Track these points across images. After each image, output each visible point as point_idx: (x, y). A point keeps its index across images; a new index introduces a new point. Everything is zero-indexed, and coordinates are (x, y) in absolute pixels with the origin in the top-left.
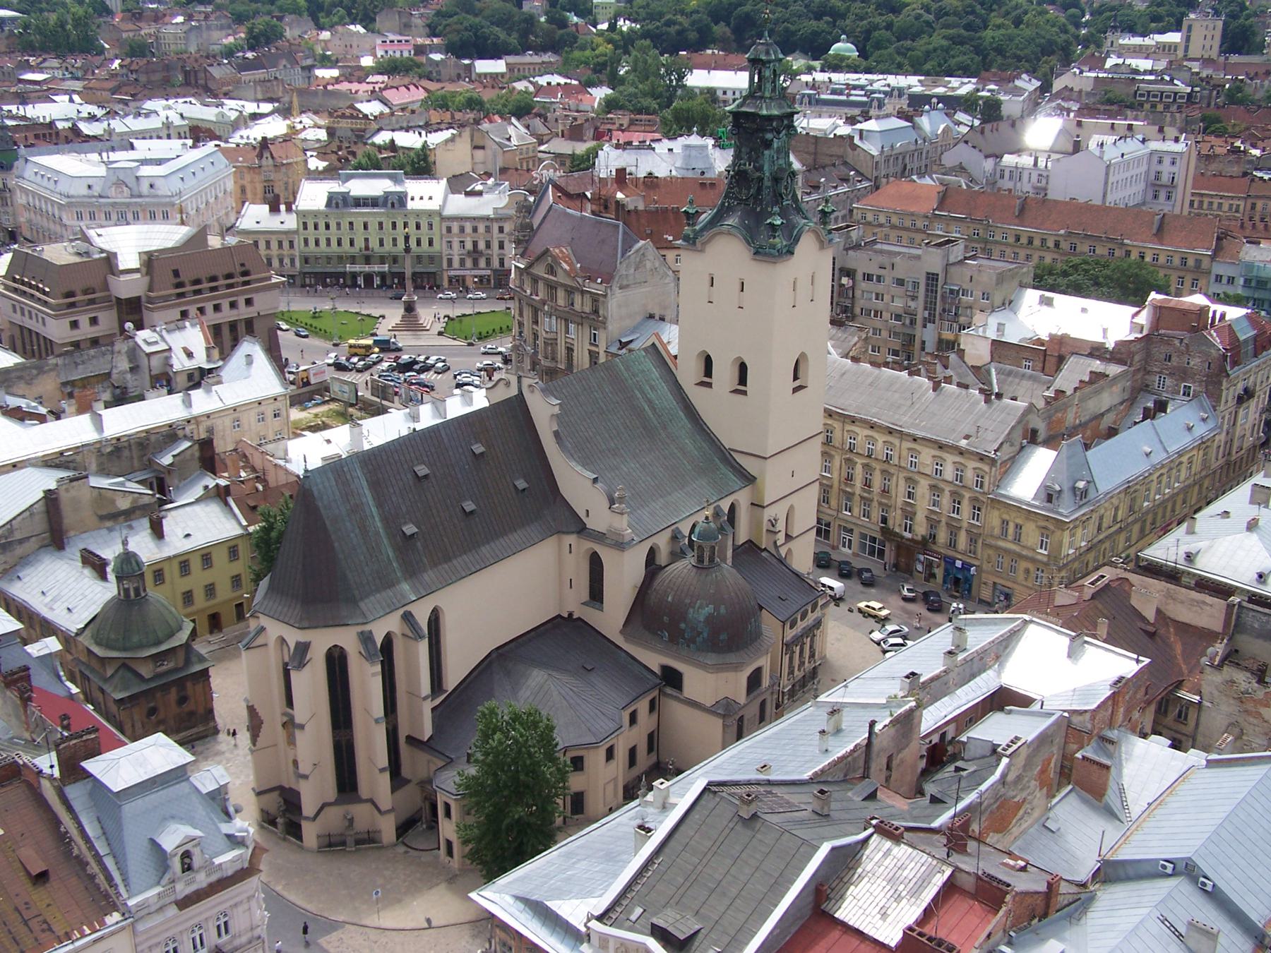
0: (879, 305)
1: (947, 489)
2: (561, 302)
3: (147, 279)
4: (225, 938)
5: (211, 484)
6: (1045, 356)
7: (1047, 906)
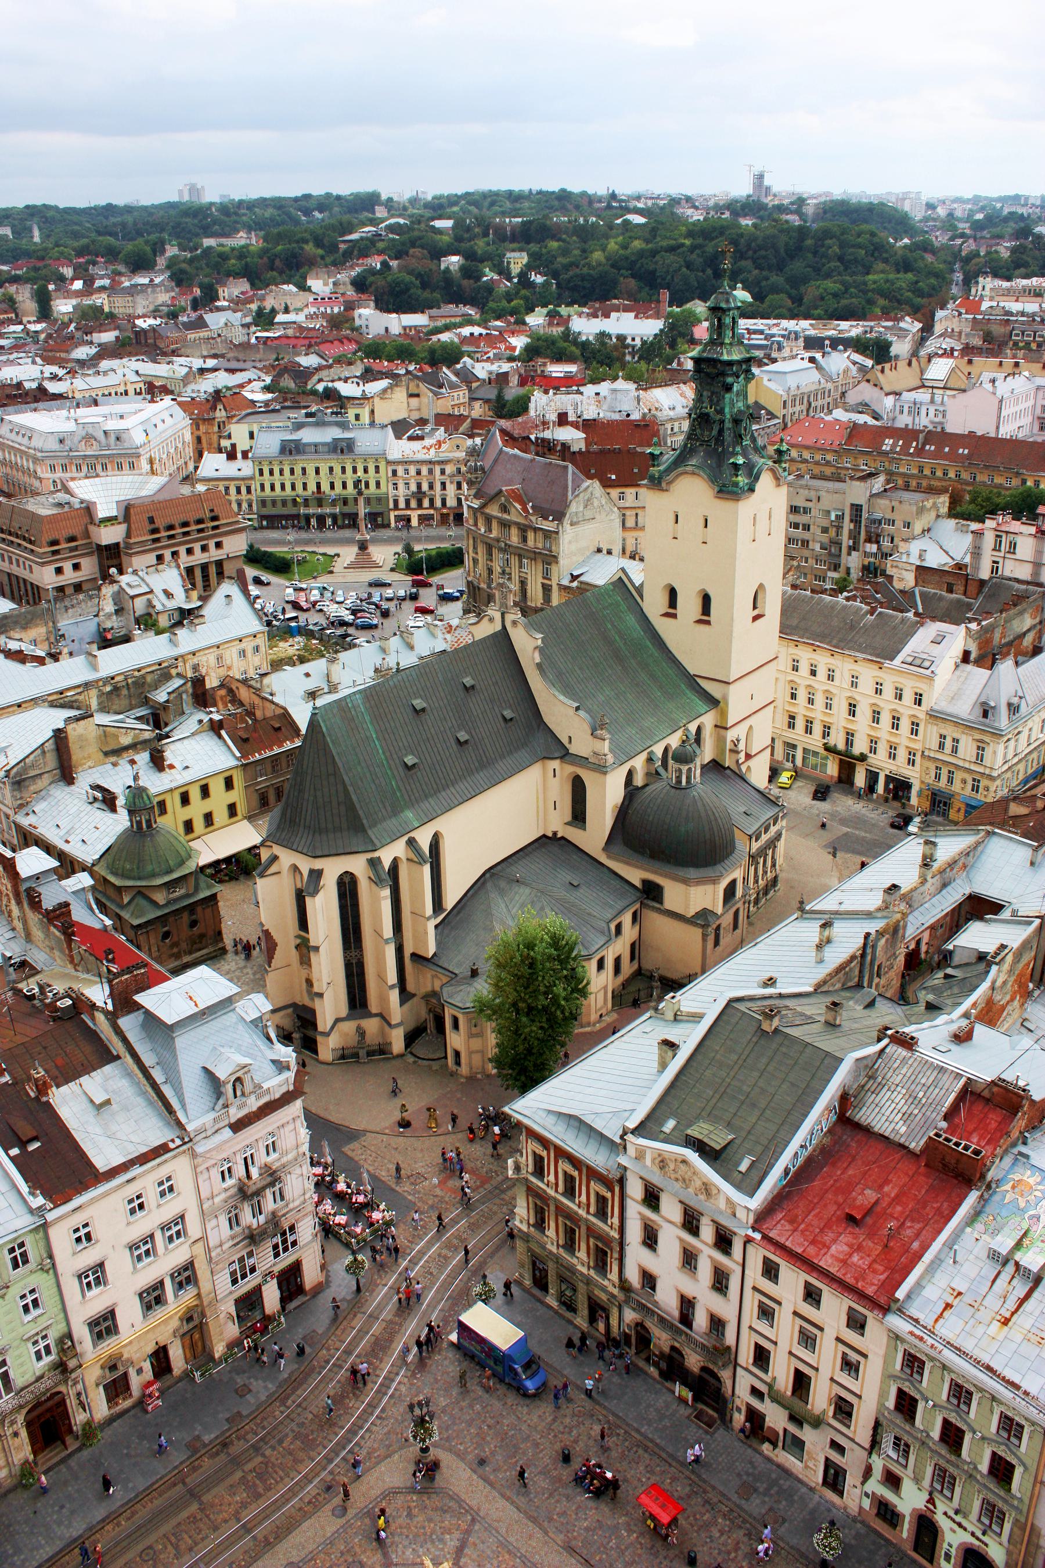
2: (515, 539)
4: (274, 1156)
5: (206, 718)
6: (967, 580)
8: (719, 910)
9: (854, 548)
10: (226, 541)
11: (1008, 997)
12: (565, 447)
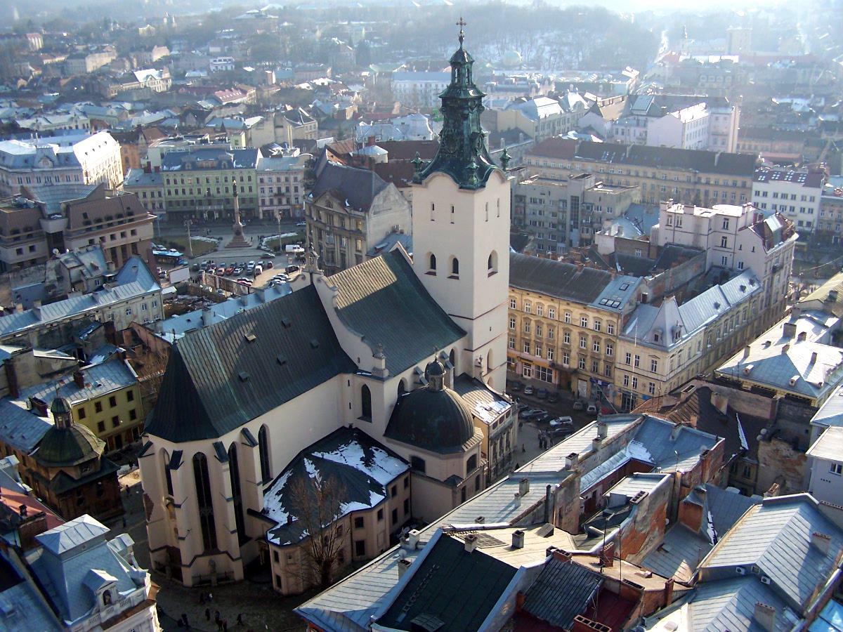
0: (542, 218)
1: (591, 334)
3: (65, 220)
7: (666, 599)
8: (464, 476)
9: (575, 226)
10: (139, 229)
11: (648, 529)
12: (372, 160)
